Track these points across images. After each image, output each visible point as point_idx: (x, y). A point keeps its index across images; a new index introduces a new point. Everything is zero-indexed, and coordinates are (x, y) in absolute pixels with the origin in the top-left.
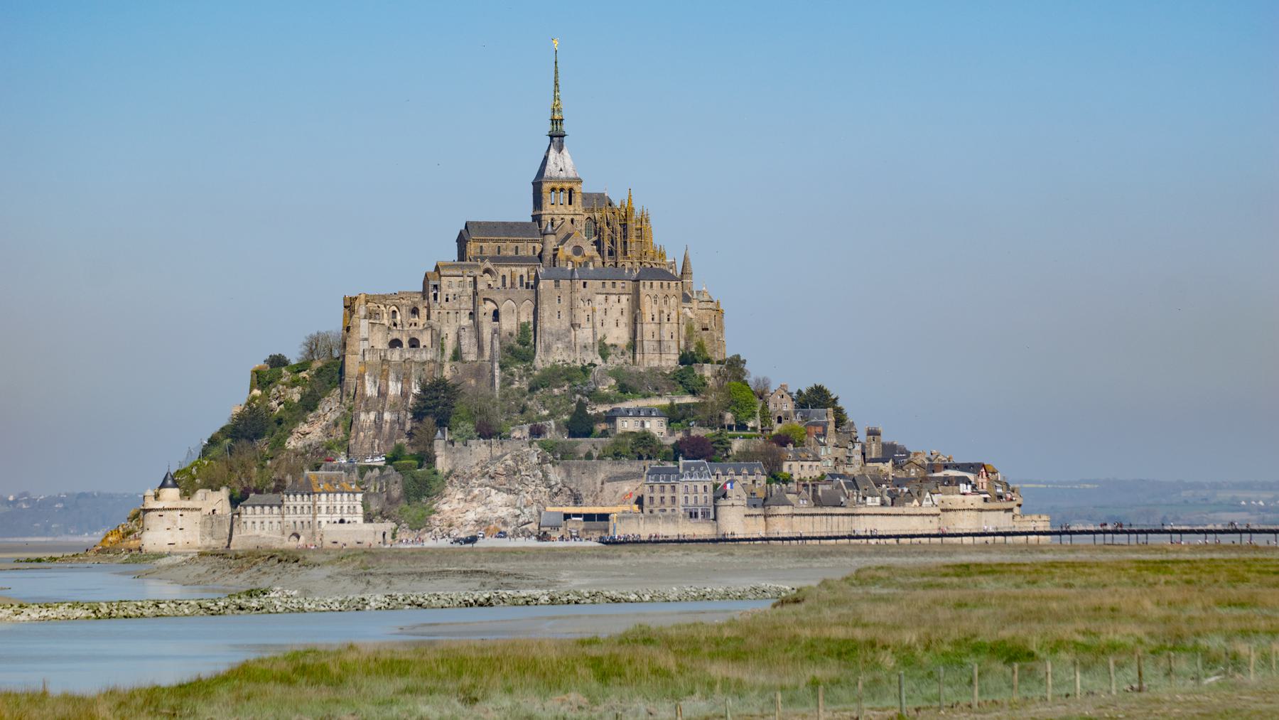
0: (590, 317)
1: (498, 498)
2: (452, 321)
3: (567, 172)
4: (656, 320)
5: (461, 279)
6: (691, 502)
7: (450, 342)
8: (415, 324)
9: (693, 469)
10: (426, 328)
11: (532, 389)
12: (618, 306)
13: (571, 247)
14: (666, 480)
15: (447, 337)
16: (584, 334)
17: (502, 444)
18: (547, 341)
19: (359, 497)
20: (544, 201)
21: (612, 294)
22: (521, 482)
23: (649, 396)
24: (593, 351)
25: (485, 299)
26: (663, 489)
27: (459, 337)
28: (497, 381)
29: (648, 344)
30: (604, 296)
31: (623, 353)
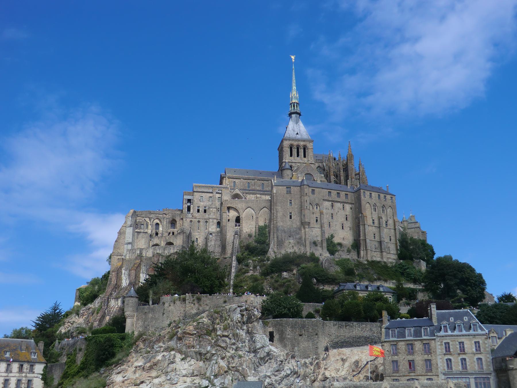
0: (319, 219)
2: (202, 228)
3: (301, 135)
5: (211, 195)
8: (173, 233)
9: (452, 319)
10: (179, 233)
17: (199, 299)
18: (280, 237)
19: (39, 368)
20: (284, 153)
22: (216, 345)
24: (322, 247)
25: (229, 208)
27: (206, 239)
28: (233, 270)
29: (371, 243)
30: (330, 203)
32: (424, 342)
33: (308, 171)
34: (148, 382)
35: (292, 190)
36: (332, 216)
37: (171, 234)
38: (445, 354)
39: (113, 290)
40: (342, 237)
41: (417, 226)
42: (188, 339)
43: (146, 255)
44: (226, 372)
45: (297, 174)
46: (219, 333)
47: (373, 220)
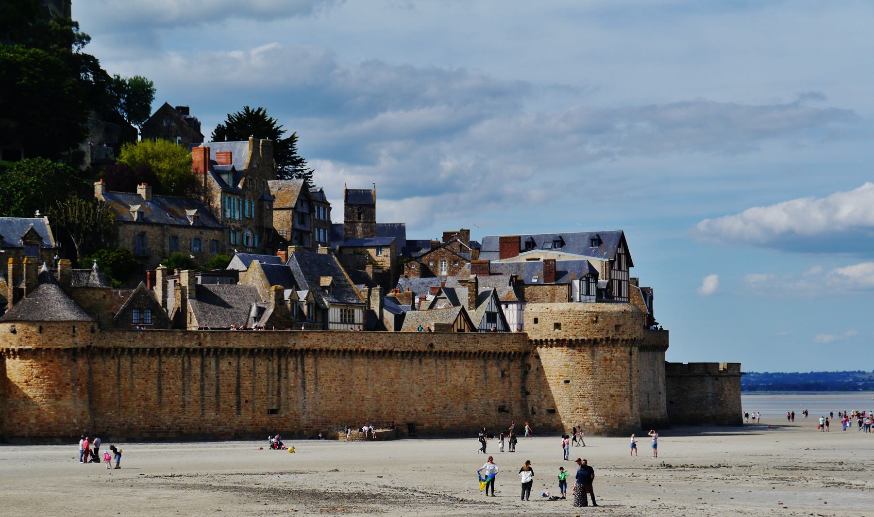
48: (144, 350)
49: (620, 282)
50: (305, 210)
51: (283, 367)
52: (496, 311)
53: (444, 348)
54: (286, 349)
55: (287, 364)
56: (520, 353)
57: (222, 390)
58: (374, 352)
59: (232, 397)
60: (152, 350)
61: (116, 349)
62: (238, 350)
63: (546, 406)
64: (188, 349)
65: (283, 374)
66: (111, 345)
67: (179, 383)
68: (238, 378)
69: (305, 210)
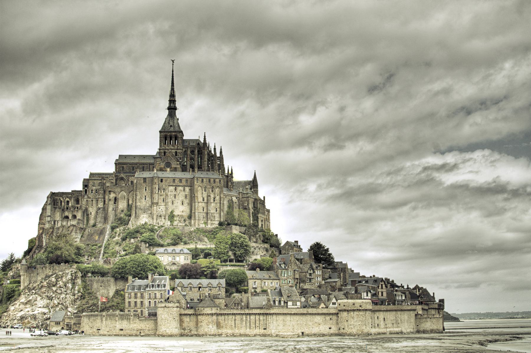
0: (165, 199)
1: (41, 302)
2: (94, 205)
3: (174, 127)
4: (205, 201)
5: (100, 181)
6: (153, 305)
7: (93, 216)
8: (78, 208)
11: (124, 239)
12: (183, 193)
13: (165, 163)
14: (138, 290)
15: (91, 214)
16: (161, 209)
17: (53, 267)
18: (138, 213)
21: (179, 186)
23: (189, 243)
24: (165, 219)
25: (110, 191)
26: (136, 297)
27: (97, 212)
30: (174, 187)
31: (185, 221)
32: (142, 293)
33: (168, 160)
34: (24, 310)
35: (147, 180)
36: (175, 197)
37: (76, 208)
38: (149, 299)
39: (36, 249)
40: (181, 210)
41: (247, 196)
42: (43, 289)
43: (57, 225)
44: (56, 306)
45: (160, 163)
46: (58, 286)
47: (203, 198)
48: (231, 314)
49: (382, 292)
50: (312, 272)
51: (267, 318)
52: (336, 301)
53: (312, 313)
54: (267, 313)
55: (269, 317)
56: (336, 314)
57: (251, 323)
58: (292, 314)
59: (254, 325)
60: (233, 314)
61: (224, 314)
62: (255, 314)
63: (342, 327)
64: (242, 314)
65: (267, 319)
66: (222, 313)
67: (240, 322)
68: (255, 320)
69: (312, 272)
